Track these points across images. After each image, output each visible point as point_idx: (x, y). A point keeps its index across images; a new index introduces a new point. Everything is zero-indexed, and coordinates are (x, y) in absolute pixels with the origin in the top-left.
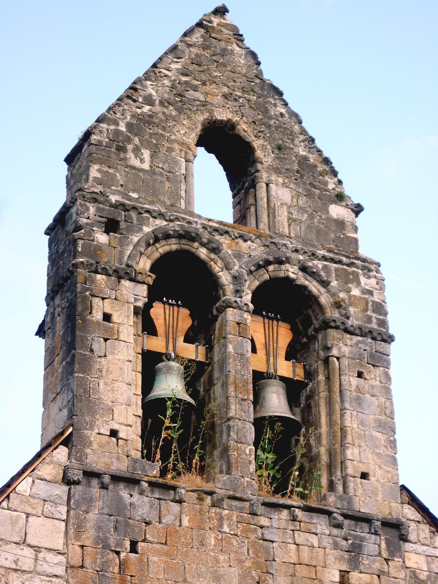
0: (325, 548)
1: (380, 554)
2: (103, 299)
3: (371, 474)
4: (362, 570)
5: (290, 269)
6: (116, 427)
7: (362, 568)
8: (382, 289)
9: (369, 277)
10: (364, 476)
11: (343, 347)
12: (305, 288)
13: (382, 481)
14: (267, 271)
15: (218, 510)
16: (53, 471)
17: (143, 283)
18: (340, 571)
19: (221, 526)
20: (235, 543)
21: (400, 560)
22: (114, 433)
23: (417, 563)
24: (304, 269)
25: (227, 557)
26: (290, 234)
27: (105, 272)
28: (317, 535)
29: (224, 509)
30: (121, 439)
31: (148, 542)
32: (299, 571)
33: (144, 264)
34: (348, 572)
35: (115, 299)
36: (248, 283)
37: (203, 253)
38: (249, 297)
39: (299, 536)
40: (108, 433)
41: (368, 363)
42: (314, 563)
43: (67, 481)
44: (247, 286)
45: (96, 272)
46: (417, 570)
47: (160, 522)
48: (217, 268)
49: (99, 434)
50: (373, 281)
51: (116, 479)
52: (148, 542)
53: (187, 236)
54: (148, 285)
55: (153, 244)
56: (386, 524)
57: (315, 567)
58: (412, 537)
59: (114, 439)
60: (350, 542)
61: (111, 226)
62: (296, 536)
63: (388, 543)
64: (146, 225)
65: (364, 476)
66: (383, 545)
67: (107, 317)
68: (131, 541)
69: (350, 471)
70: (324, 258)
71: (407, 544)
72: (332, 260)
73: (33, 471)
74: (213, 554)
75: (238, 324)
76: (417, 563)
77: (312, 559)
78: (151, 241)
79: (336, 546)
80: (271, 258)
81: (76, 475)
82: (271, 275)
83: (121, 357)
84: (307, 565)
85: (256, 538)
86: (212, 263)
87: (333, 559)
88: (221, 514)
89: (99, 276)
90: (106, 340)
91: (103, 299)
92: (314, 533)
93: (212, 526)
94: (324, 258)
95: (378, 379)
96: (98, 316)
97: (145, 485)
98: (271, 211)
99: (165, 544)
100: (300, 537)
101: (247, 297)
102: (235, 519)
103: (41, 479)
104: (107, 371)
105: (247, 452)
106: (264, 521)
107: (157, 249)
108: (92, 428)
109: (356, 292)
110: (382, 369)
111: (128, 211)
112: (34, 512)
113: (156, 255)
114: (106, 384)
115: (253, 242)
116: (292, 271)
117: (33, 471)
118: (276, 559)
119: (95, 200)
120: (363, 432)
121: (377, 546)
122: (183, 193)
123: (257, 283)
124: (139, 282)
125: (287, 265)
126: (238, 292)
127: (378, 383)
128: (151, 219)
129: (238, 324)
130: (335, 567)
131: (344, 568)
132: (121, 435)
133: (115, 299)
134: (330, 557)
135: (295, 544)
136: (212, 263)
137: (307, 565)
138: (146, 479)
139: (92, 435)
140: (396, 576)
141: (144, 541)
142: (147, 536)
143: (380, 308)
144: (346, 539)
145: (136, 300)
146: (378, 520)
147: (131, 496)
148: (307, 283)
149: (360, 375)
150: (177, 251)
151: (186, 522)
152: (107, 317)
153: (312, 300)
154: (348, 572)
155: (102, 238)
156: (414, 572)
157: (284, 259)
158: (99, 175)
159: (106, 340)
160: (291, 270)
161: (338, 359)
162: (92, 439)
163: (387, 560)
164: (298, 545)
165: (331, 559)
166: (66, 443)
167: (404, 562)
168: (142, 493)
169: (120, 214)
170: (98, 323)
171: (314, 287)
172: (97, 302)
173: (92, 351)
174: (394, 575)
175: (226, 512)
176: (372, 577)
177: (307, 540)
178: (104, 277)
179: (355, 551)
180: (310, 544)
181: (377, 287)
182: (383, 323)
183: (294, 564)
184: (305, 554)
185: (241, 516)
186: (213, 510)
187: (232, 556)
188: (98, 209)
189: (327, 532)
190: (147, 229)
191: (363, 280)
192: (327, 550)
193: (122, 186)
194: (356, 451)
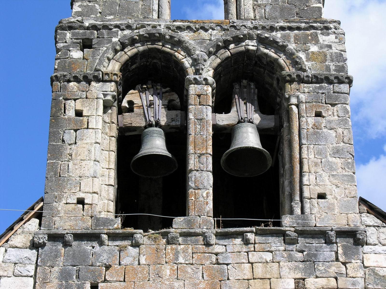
0: (279, 262)
1: (337, 259)
2: (75, 100)
3: (328, 193)
4: (318, 275)
5: (250, 43)
6: (81, 195)
7: (318, 273)
8: (341, 41)
9: (328, 34)
10: (322, 196)
11: (299, 95)
12: (266, 55)
13: (339, 198)
14: (229, 50)
15: (174, 246)
16: (24, 239)
17: (111, 81)
18: (295, 279)
19: (177, 259)
20: (189, 270)
21: (359, 261)
22: (81, 201)
23: (377, 261)
24: (262, 41)
25: (181, 283)
26: (255, 17)
27: (76, 79)
28: (272, 252)
29: (179, 244)
30: (87, 204)
31: (108, 281)
32: (253, 285)
33: (114, 67)
34: (304, 279)
35: (87, 98)
36: (208, 63)
37: (167, 48)
38: (211, 73)
39: (253, 255)
40: (75, 201)
41: (326, 104)
42: (268, 276)
43: (35, 246)
44: (209, 64)
45: (69, 81)
46: (376, 268)
47: (120, 264)
48: (180, 55)
49: (67, 204)
50: (332, 37)
51: (79, 237)
52: (108, 281)
53: (152, 38)
54: (116, 82)
55: (122, 50)
56: (342, 234)
57: (270, 279)
58: (372, 239)
59: (81, 206)
60: (305, 253)
61: (86, 44)
62: (250, 256)
63: (345, 248)
64: (115, 37)
65: (322, 196)
66: (340, 251)
67: (79, 114)
68: (91, 284)
69: (306, 194)
70: (282, 29)
71: (365, 247)
72: (291, 29)
73: (7, 241)
74: (168, 283)
75: (199, 96)
76: (377, 261)
77: (266, 273)
78: (118, 48)
79: (290, 259)
80: (229, 38)
81: (43, 239)
82: (231, 51)
83: (88, 141)
84: (261, 279)
85: (211, 263)
86: (176, 54)
87: (288, 270)
88: (176, 249)
89: (72, 84)
90: (76, 131)
91: (75, 100)
92: (268, 251)
93: (167, 260)
94: (282, 29)
95: (335, 114)
96: (71, 113)
97: (105, 237)
98: (238, 3)
99: (124, 281)
100: (253, 257)
101: (208, 74)
102: (190, 251)
103: (13, 248)
104: (76, 154)
105: (205, 195)
106: (218, 249)
107: (125, 53)
108: (60, 199)
109: (314, 48)
110: (339, 105)
111: (100, 29)
112: (5, 274)
113: (125, 58)
114: (75, 164)
115: (213, 29)
116: (252, 45)
117: (7, 241)
118: (230, 278)
119: (70, 28)
120: (320, 161)
121: (333, 253)
122: (156, 7)
123: (218, 61)
124: (106, 81)
125: (247, 41)
126: (197, 72)
127: (336, 117)
128: (120, 32)
129: (199, 96)
130: (290, 277)
131: (299, 276)
132: (86, 201)
133: (87, 98)
134: (284, 269)
135: (249, 262)
136: (176, 54)
137: (261, 279)
138: (106, 231)
139: (60, 206)
140: (354, 276)
141: (105, 281)
142: (107, 277)
143: (340, 57)
144: (302, 252)
145: (105, 95)
146: (332, 230)
147: (93, 247)
148: (266, 51)
149: (318, 115)
150: (144, 51)
151: (143, 260)
152: (79, 114)
153: (274, 65)
154: (304, 279)
155: (76, 54)
156: (373, 271)
157: (242, 36)
158: (80, 10)
159: (76, 131)
160: (250, 43)
161: (297, 106)
162: (60, 209)
163: (344, 264)
164: (252, 264)
165: (285, 271)
166: (39, 216)
167: (363, 263)
168: (101, 244)
169: (92, 34)
170: (69, 119)
171: (271, 53)
172: (71, 103)
173: (63, 141)
174: (351, 275)
175: (182, 246)
176: (328, 280)
177: (261, 258)
178: (75, 83)
179: (310, 261)
180: (264, 261)
181: (337, 40)
182: (343, 69)
183: (248, 280)
184: (259, 270)
185: (196, 248)
186: (169, 247)
187: (187, 282)
188: (73, 35)
189: (282, 248)
190: (115, 40)
191: (322, 38)
192: (281, 263)
193: (100, 13)
194: (312, 177)
